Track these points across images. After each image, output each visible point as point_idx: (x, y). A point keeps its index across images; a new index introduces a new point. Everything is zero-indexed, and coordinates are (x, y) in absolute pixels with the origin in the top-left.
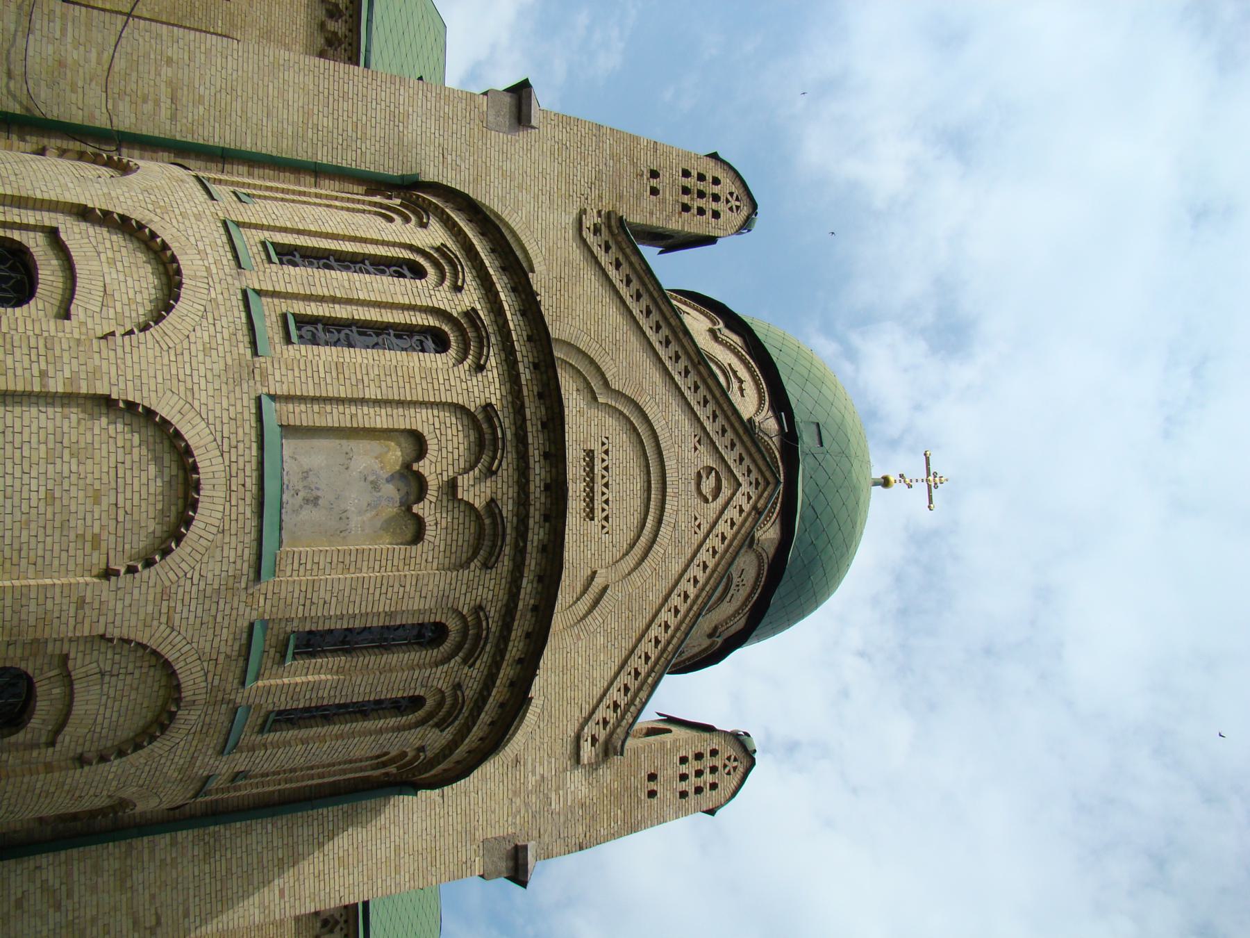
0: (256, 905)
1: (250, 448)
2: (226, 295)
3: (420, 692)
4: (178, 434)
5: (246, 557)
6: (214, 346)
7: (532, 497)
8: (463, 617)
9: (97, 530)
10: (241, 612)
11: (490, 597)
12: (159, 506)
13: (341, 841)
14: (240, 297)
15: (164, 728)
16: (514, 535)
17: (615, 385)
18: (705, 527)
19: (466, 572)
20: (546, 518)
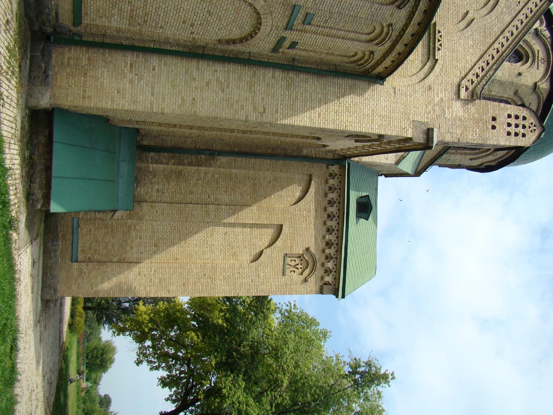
0: (308, 117)
13: (347, 99)
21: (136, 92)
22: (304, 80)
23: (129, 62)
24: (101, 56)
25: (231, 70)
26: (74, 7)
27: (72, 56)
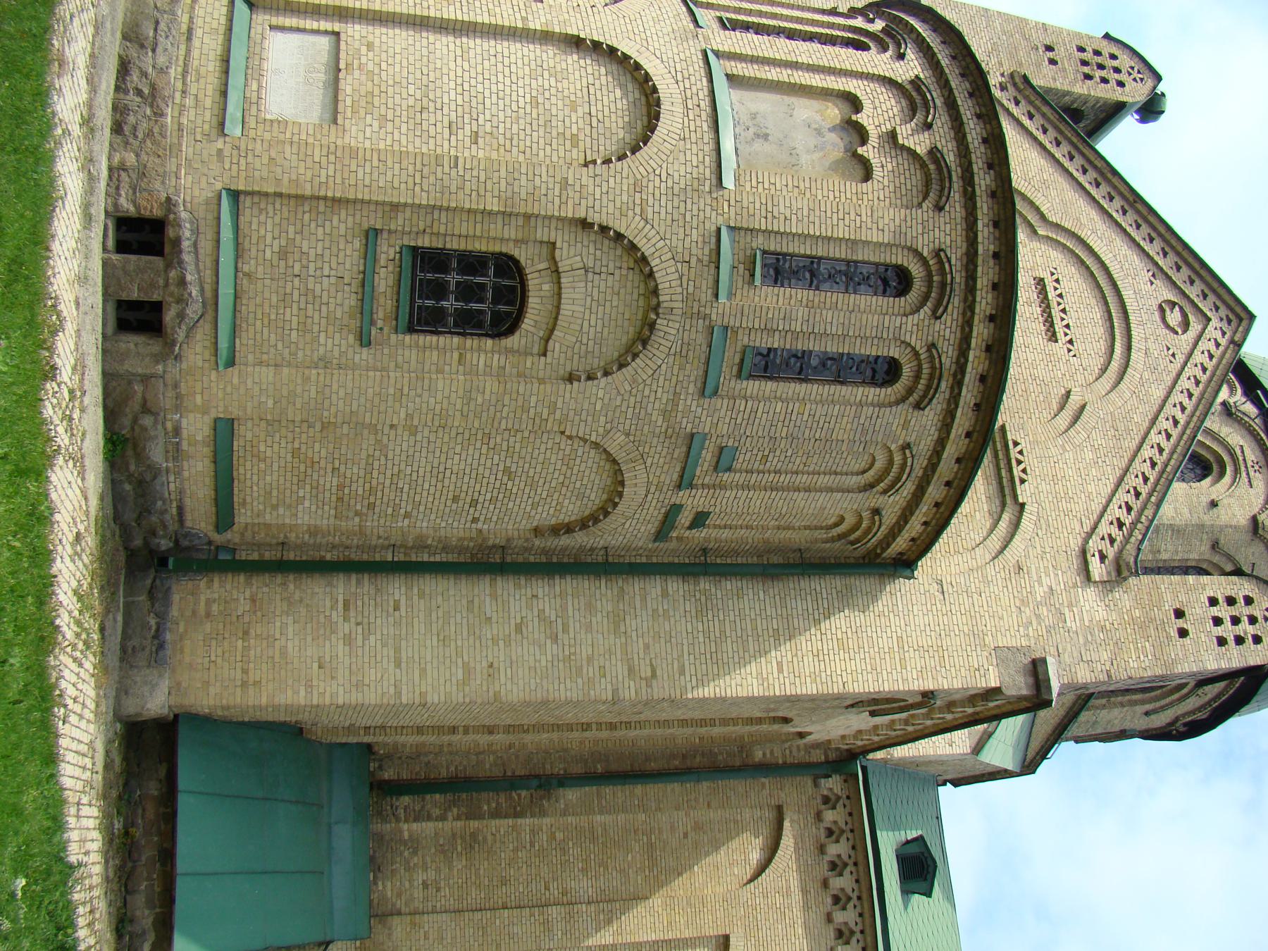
0: (754, 675)
3: (895, 352)
4: (638, 66)
5: (707, 163)
7: (971, 146)
8: (924, 261)
9: (575, 131)
10: (708, 215)
11: (948, 243)
12: (626, 119)
15: (645, 343)
18: (1180, 358)
21: (360, 663)
22: (735, 591)
23: (341, 598)
24: (279, 590)
25: (570, 591)
26: (216, 490)
27: (216, 596)
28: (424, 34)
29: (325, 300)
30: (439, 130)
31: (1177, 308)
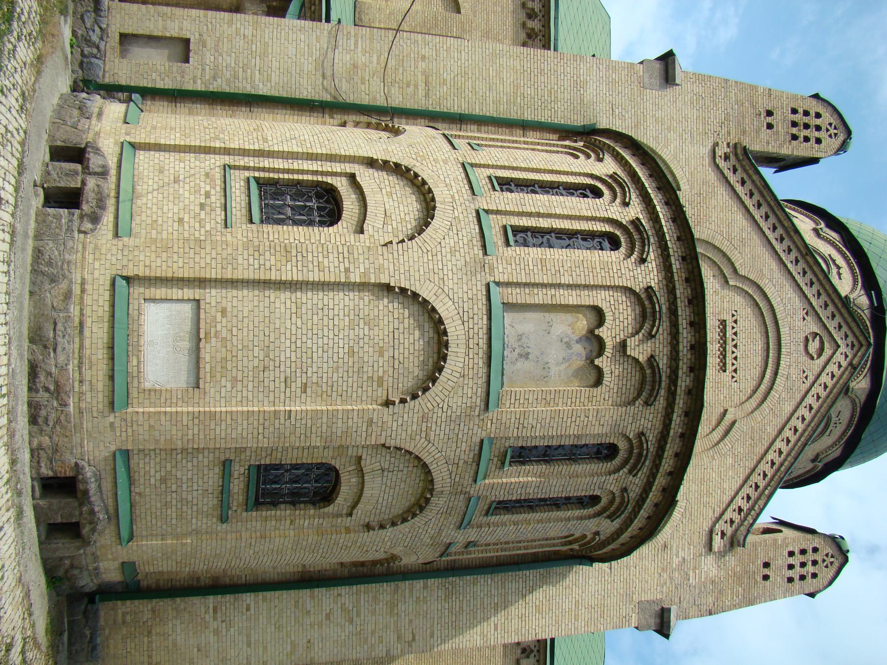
1: (482, 319)
2: (465, 214)
3: (597, 492)
4: (434, 310)
5: (479, 394)
6: (457, 249)
7: (681, 354)
8: (630, 440)
9: (381, 374)
11: (649, 426)
12: (421, 358)
14: (474, 215)
15: (422, 509)
16: (668, 382)
17: (742, 272)
18: (811, 378)
19: (632, 408)
20: (691, 369)
21: (224, 645)
27: (129, 610)
28: (267, 293)
29: (195, 501)
30: (277, 385)
31: (818, 338)
